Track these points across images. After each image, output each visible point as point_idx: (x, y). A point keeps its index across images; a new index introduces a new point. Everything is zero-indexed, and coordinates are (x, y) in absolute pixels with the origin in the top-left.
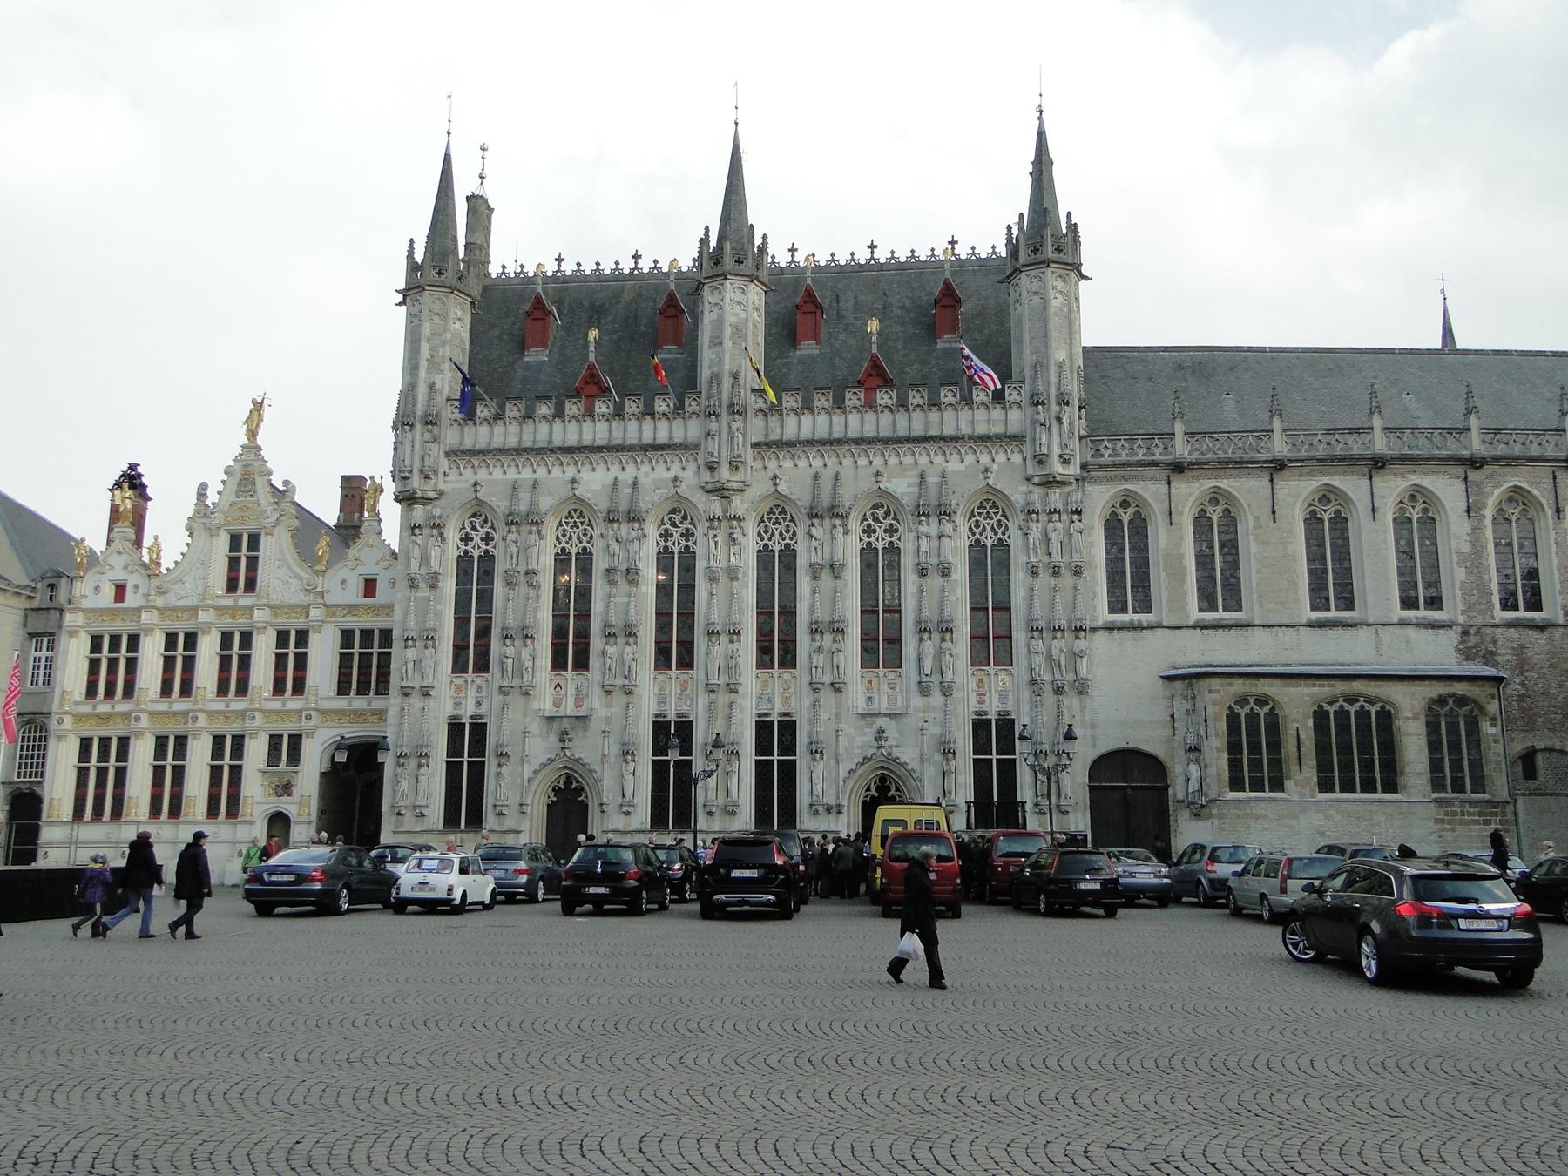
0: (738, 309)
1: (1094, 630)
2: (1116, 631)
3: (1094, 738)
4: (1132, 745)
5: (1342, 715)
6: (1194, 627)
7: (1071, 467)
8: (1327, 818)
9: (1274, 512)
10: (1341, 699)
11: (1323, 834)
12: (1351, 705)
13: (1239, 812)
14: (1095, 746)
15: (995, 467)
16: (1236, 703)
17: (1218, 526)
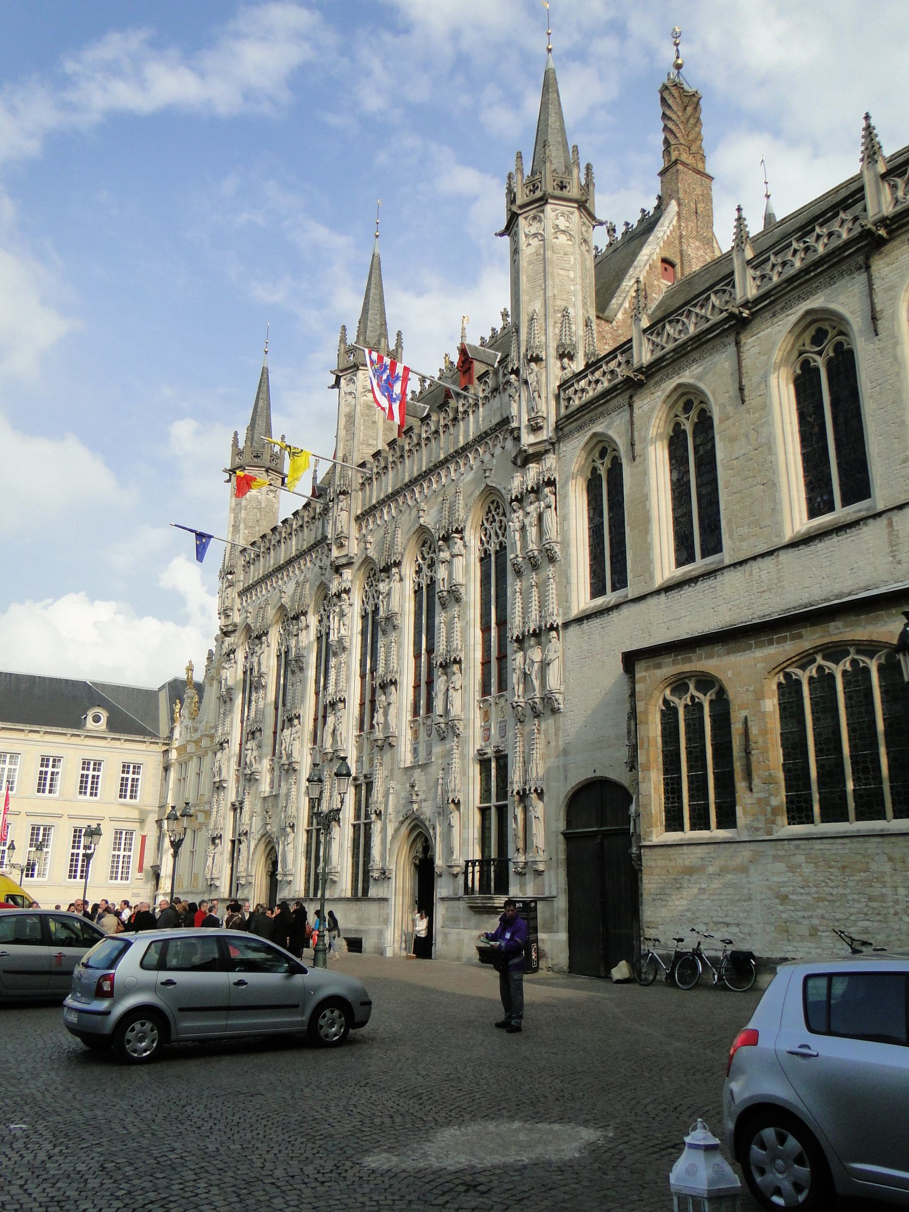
0: (349, 398)
1: (566, 625)
2: (585, 621)
3: (565, 769)
4: (598, 774)
5: (824, 681)
6: (658, 592)
7: (545, 431)
8: (792, 869)
9: (741, 389)
10: (820, 660)
11: (784, 899)
12: (837, 663)
13: (669, 864)
14: (566, 777)
15: (494, 462)
16: (673, 692)
17: (694, 437)
